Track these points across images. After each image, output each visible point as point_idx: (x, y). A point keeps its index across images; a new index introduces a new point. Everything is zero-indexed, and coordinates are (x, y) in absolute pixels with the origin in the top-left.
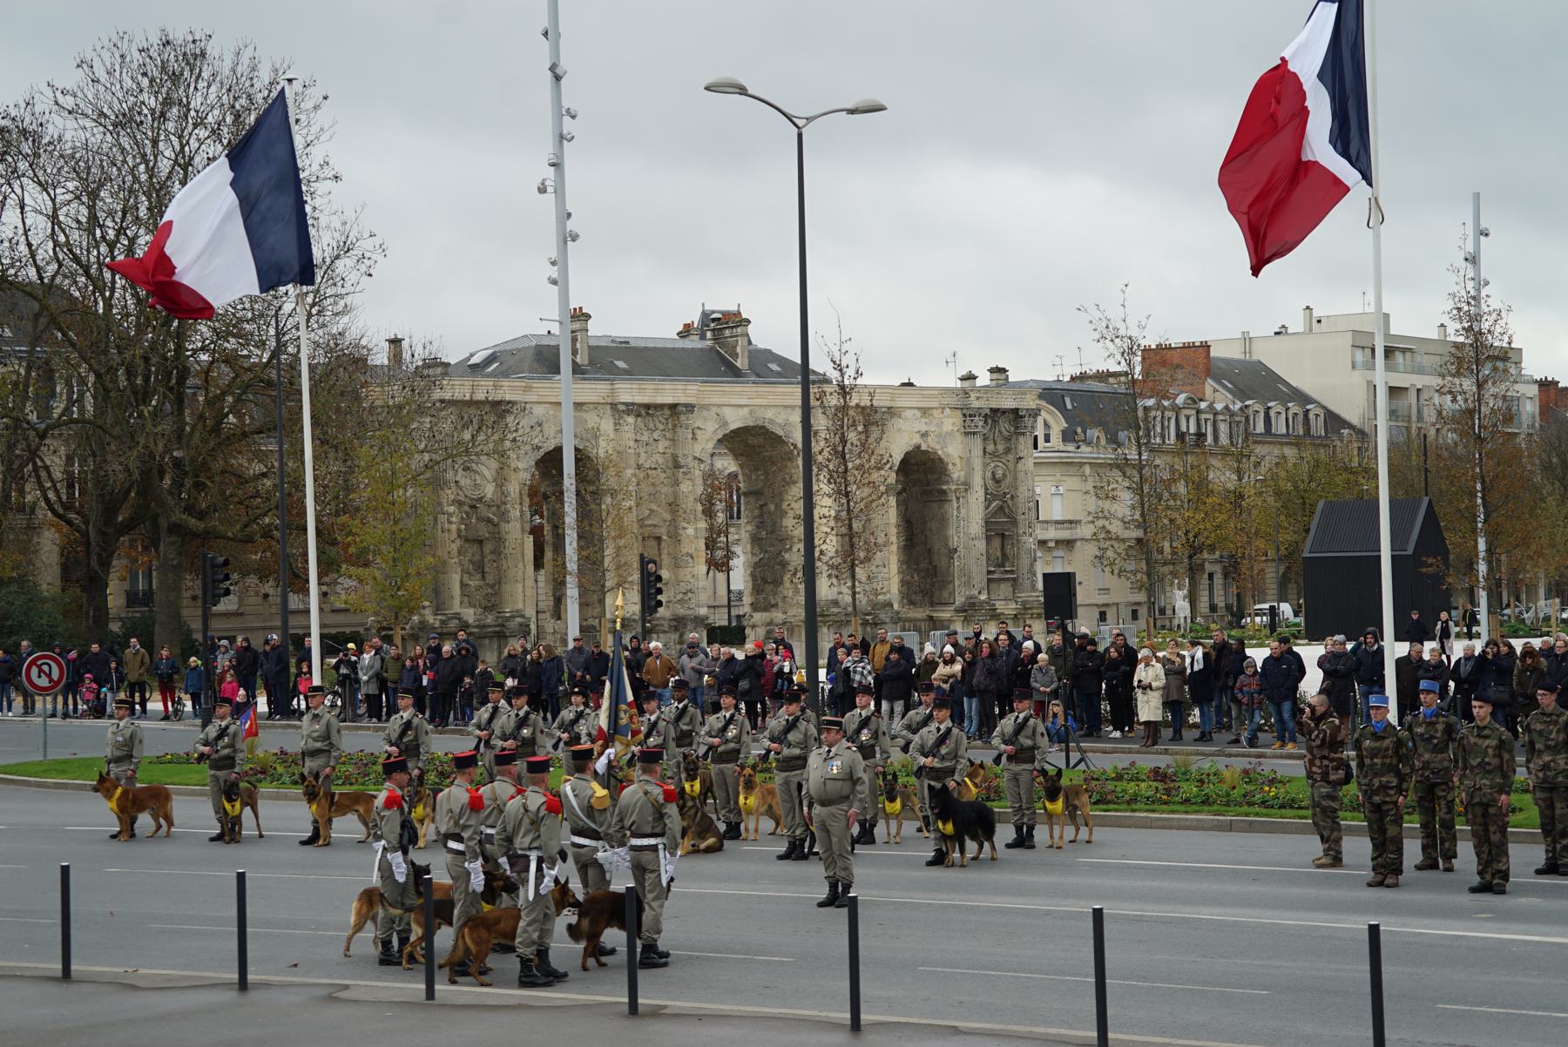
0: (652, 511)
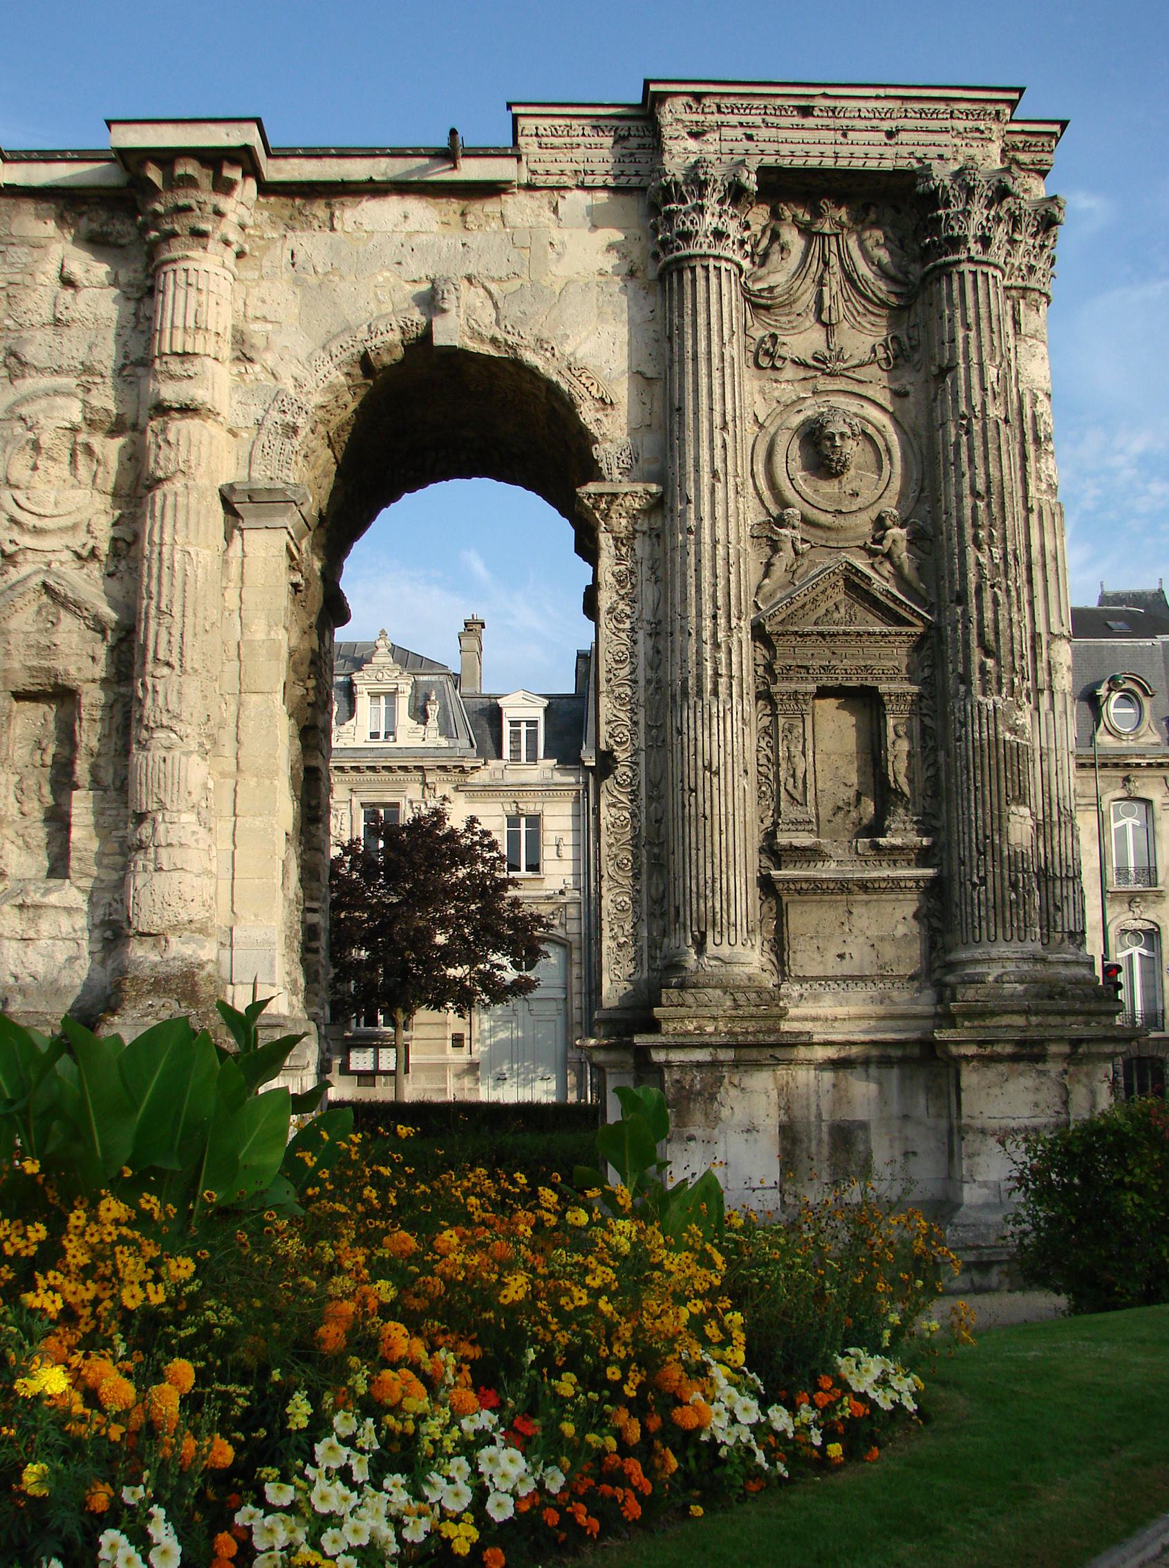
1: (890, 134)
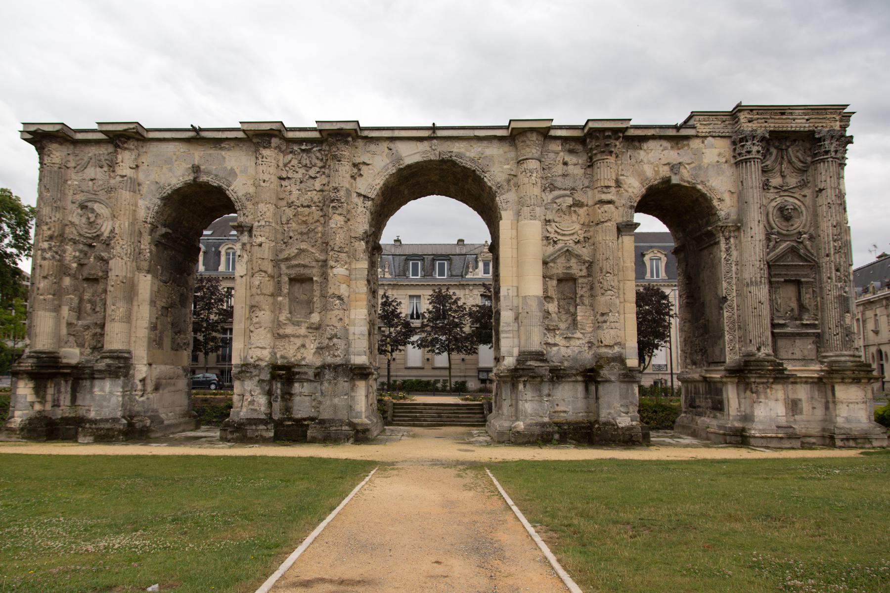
0: (301, 251)
1: (807, 120)
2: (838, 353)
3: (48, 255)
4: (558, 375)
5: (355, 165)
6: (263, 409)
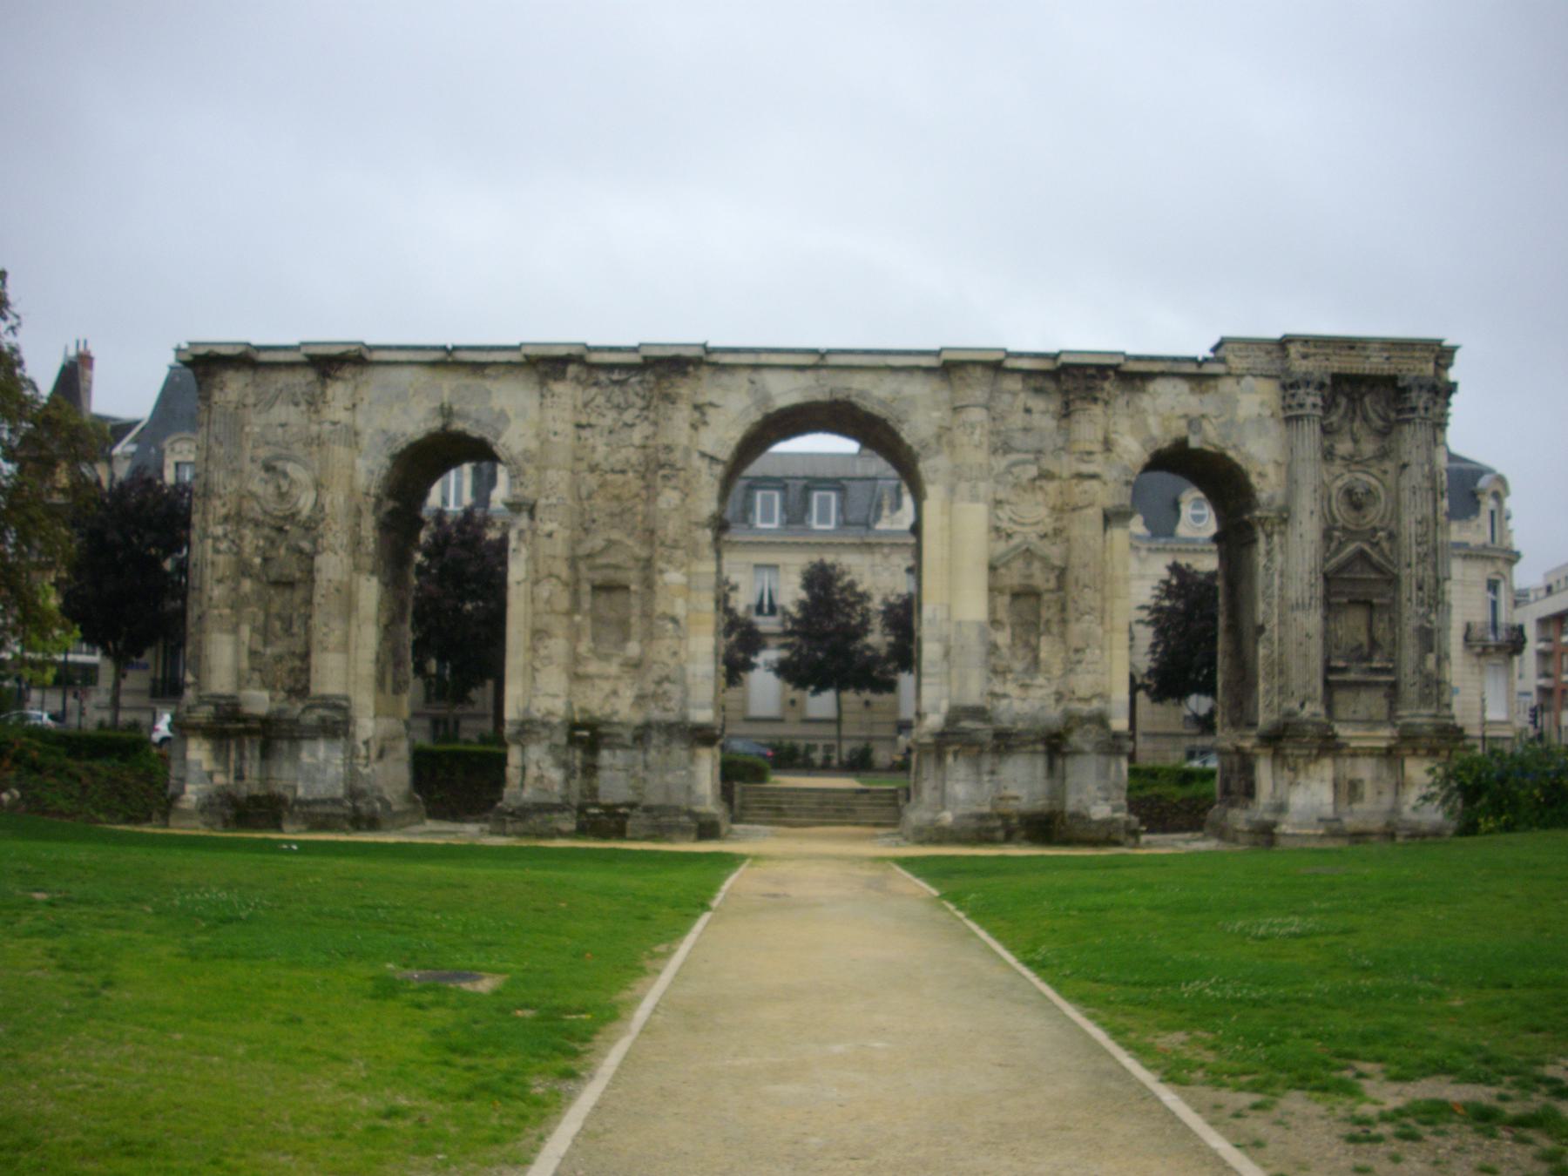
0: (611, 543)
1: (1388, 358)
2: (1414, 711)
3: (223, 546)
4: (1005, 742)
5: (697, 407)
6: (557, 788)
